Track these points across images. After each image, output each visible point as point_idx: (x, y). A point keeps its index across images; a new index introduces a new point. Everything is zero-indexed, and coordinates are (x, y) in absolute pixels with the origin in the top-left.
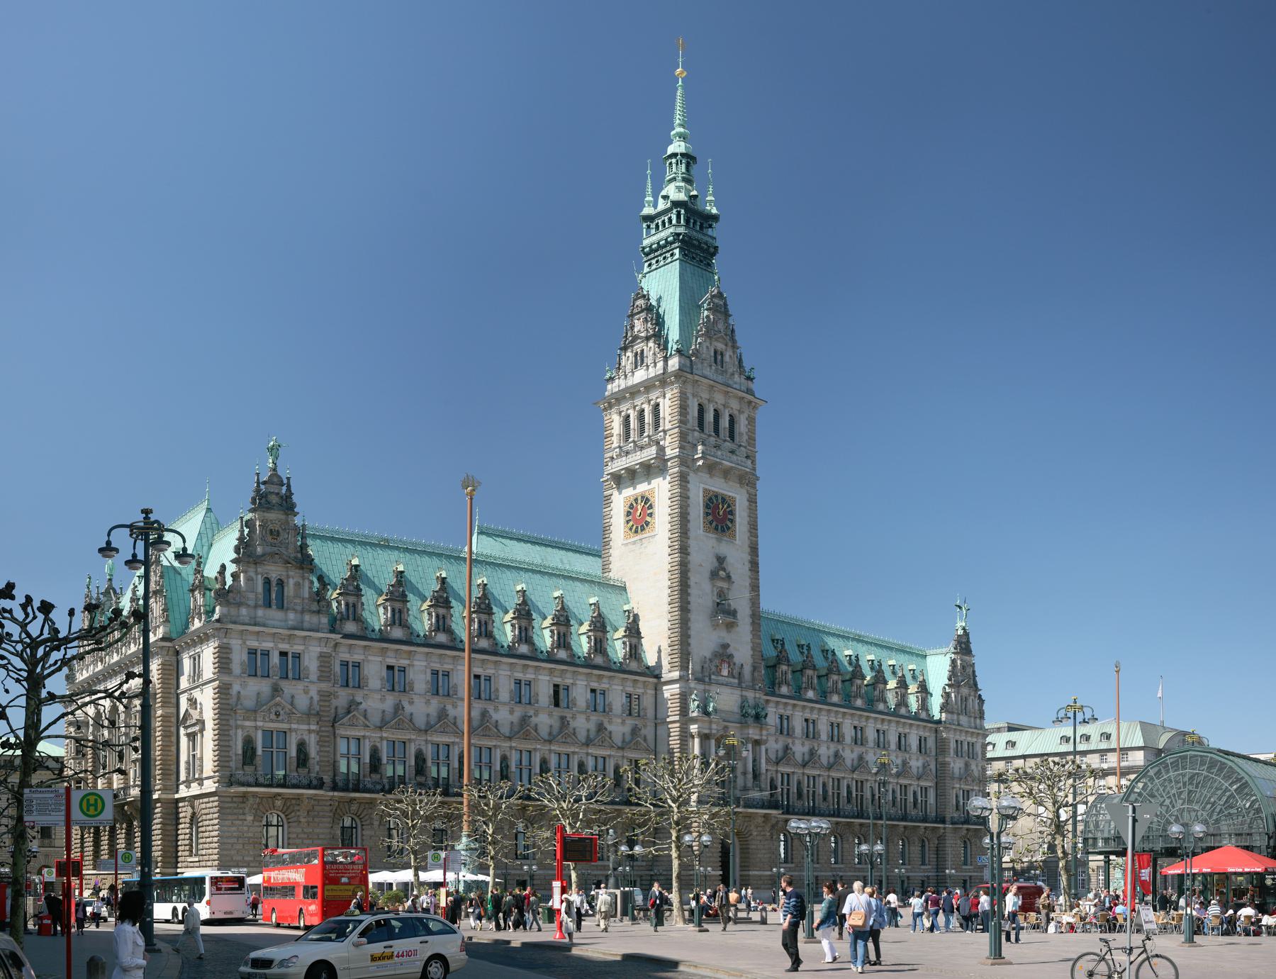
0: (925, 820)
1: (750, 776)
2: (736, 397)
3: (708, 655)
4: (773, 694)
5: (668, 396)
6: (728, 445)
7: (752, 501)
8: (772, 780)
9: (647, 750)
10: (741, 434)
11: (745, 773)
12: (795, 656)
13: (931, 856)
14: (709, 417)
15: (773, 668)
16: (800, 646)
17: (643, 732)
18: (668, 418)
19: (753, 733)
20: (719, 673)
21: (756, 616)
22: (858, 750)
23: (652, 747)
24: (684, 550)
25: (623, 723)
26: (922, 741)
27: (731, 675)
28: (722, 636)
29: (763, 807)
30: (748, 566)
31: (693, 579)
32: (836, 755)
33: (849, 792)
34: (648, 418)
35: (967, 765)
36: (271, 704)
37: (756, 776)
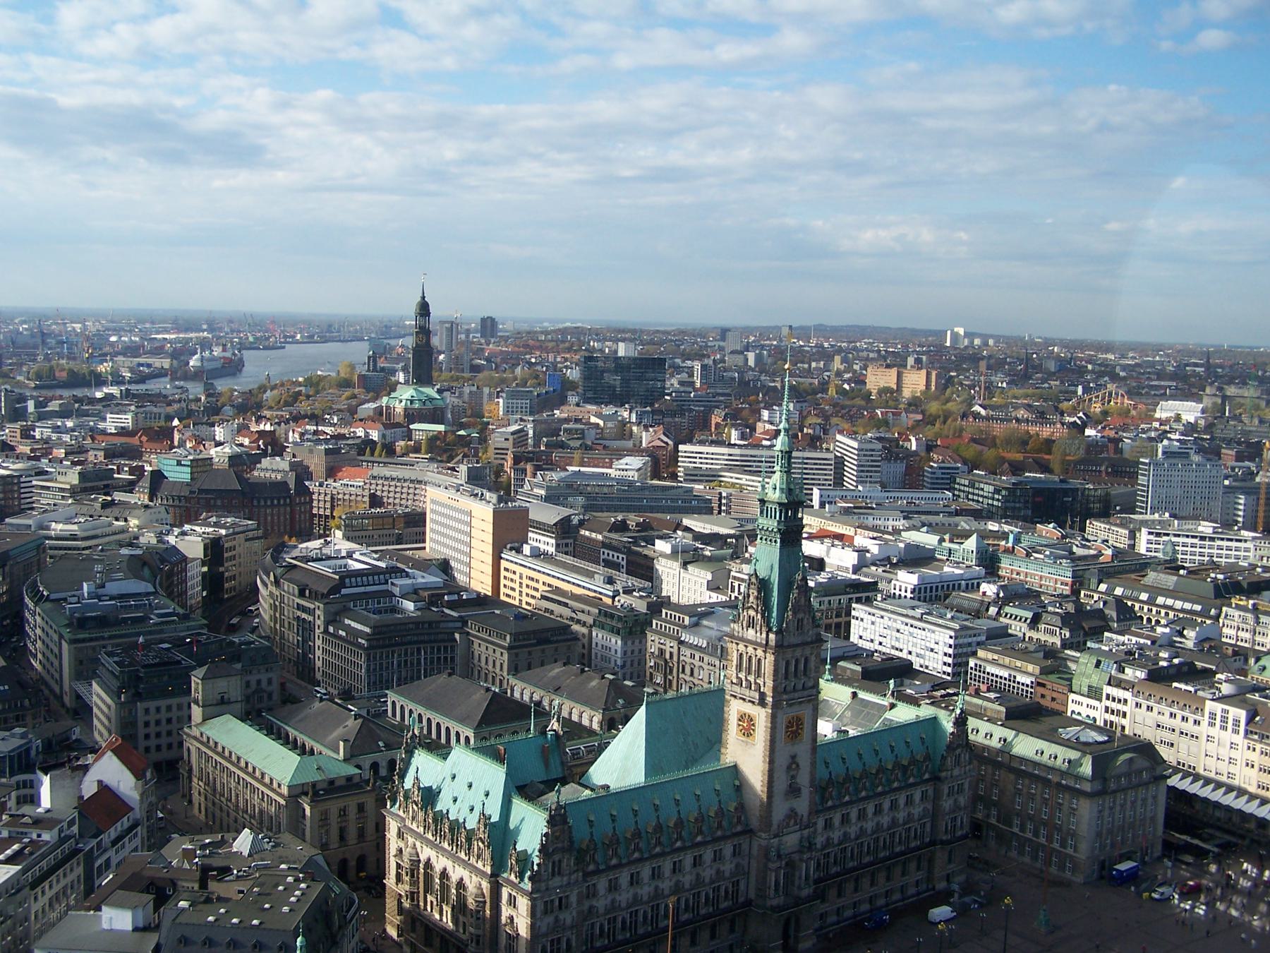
11: (800, 878)
13: (925, 864)
24: (771, 762)
27: (796, 824)
31: (776, 776)
35: (956, 800)
36: (557, 926)
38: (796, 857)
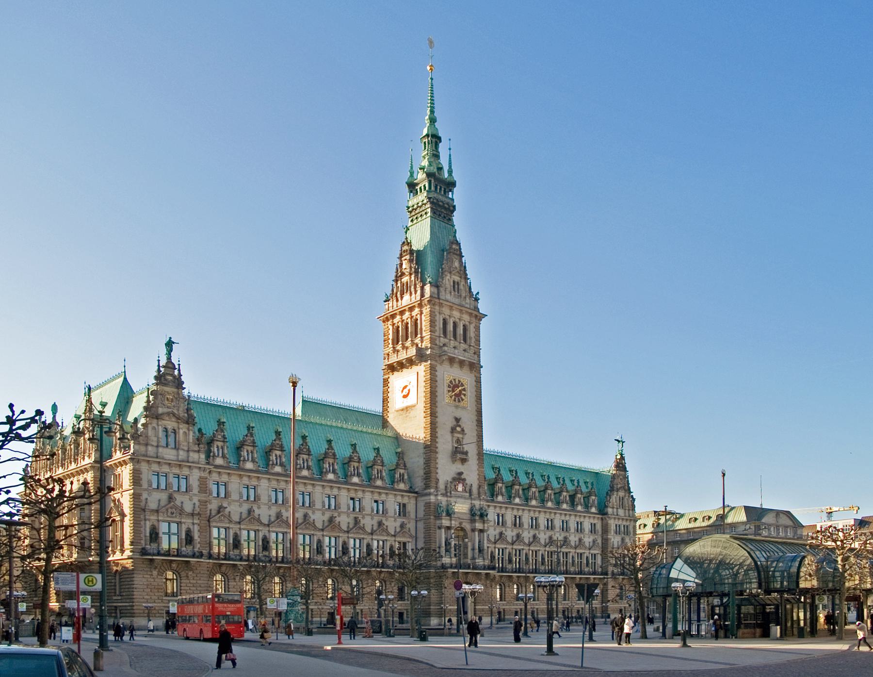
0: (594, 573)
1: (477, 551)
2: (467, 312)
3: (450, 480)
4: (493, 501)
6: (463, 346)
7: (478, 381)
8: (492, 553)
9: (411, 536)
10: (470, 338)
12: (507, 477)
14: (450, 327)
15: (492, 485)
16: (511, 471)
17: (408, 526)
19: (479, 526)
20: (456, 490)
21: (481, 454)
22: (549, 533)
23: (414, 534)
25: (395, 520)
26: (593, 526)
27: (465, 490)
28: (458, 467)
29: (484, 569)
30: (475, 423)
31: (440, 432)
32: (534, 537)
33: (543, 559)
37: (481, 550)
38: (467, 526)
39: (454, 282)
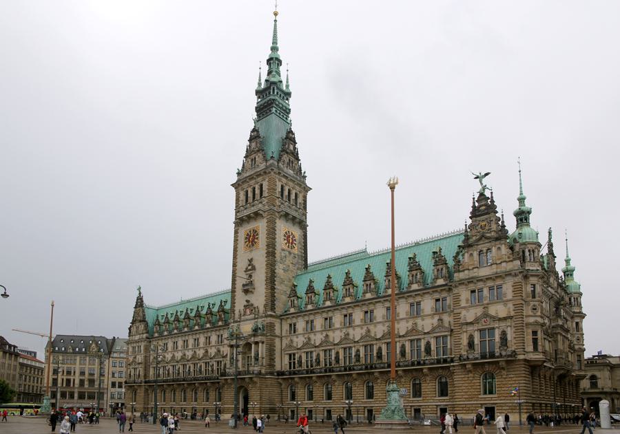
5: (267, 180)
14: (286, 193)
18: (267, 191)
34: (257, 192)
39: (289, 160)
